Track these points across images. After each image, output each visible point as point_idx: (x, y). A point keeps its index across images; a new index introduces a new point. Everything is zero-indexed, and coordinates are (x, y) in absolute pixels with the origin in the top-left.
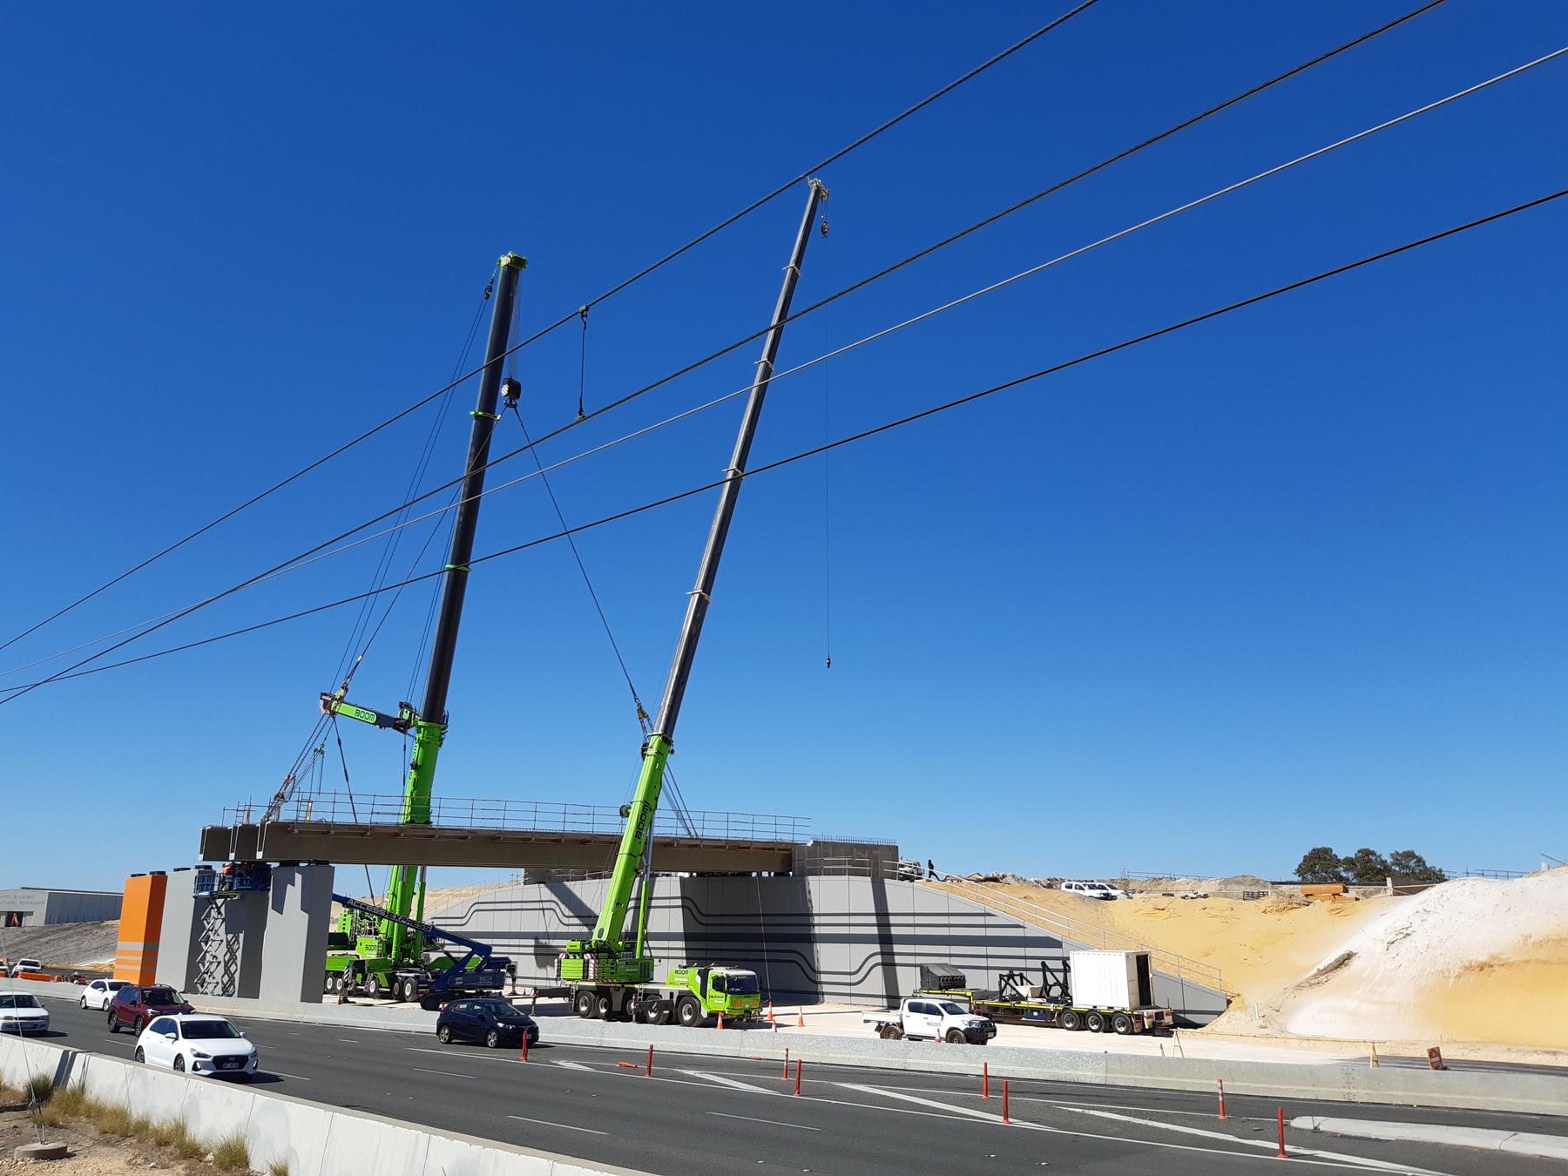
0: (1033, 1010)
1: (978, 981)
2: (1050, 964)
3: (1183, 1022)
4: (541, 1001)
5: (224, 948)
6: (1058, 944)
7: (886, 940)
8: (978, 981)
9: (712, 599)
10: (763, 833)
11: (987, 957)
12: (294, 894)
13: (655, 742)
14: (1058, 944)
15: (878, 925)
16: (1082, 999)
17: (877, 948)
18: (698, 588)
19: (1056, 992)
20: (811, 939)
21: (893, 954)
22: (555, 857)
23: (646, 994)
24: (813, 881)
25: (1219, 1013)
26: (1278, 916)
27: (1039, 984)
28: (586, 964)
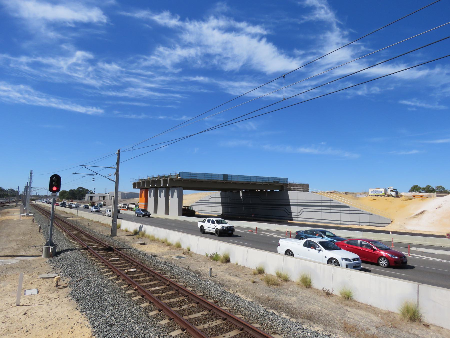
14: (348, 207)
25: (389, 224)
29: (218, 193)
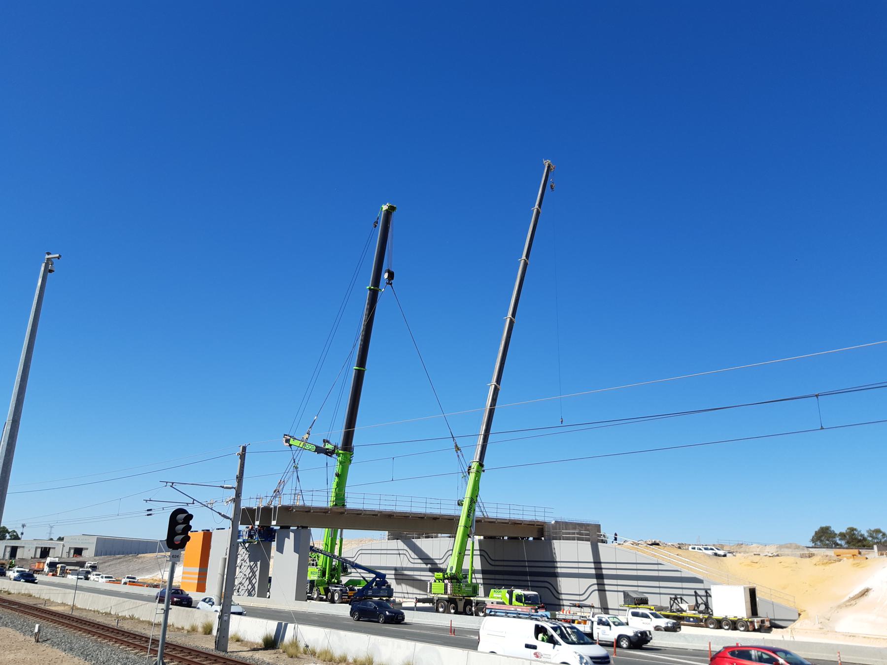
0: (690, 617)
3: (774, 626)
4: (420, 605)
5: (249, 570)
6: (701, 581)
7: (600, 576)
8: (653, 600)
9: (501, 387)
10: (528, 516)
12: (289, 543)
13: (475, 466)
14: (701, 581)
15: (595, 568)
16: (718, 613)
17: (595, 581)
18: (494, 382)
20: (555, 575)
21: (604, 585)
22: (404, 526)
23: (478, 603)
24: (556, 544)
26: (823, 567)
27: (694, 603)
28: (446, 586)
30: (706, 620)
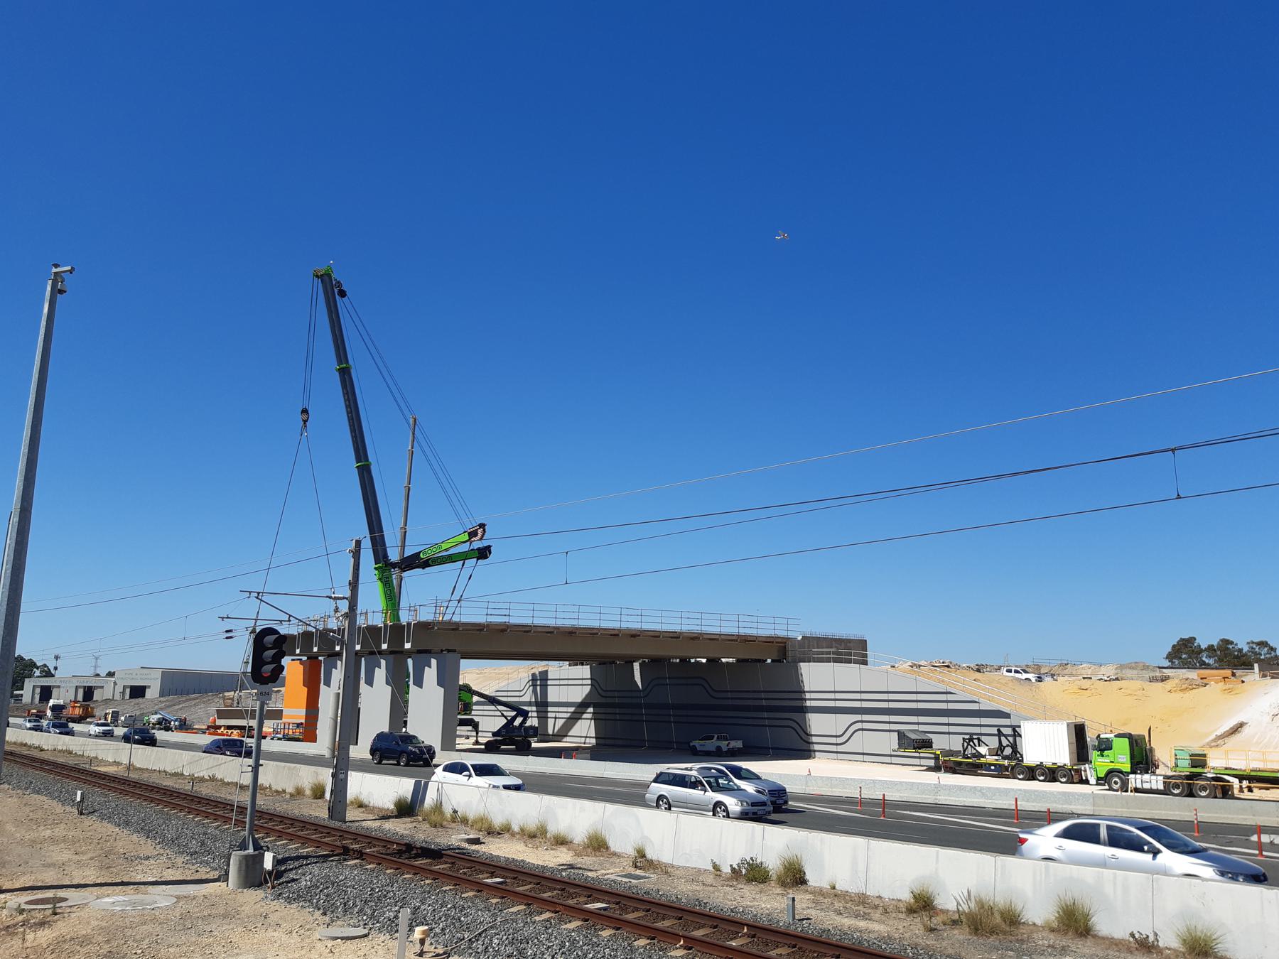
1: (940, 743)
2: (1004, 731)
6: (1007, 716)
8: (940, 743)
10: (765, 631)
11: (949, 725)
14: (1007, 716)
19: (1008, 751)
20: (804, 710)
26: (1181, 694)
29: (584, 671)
30: (1013, 768)
